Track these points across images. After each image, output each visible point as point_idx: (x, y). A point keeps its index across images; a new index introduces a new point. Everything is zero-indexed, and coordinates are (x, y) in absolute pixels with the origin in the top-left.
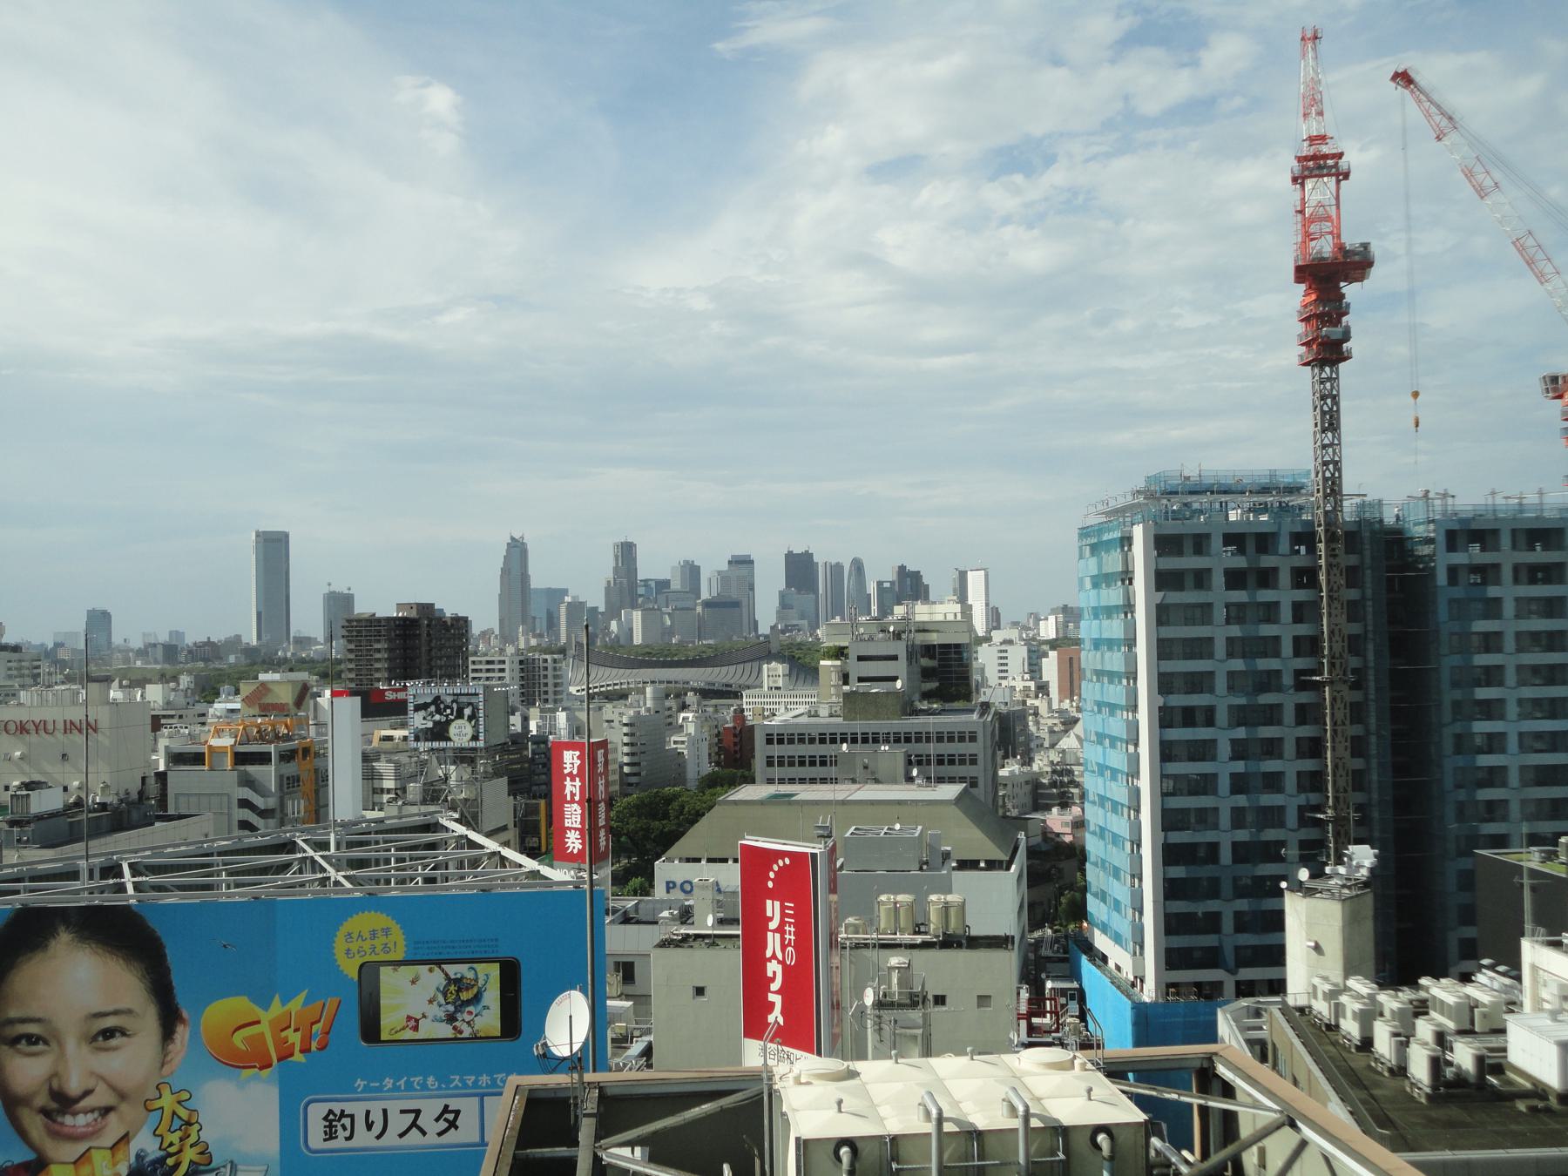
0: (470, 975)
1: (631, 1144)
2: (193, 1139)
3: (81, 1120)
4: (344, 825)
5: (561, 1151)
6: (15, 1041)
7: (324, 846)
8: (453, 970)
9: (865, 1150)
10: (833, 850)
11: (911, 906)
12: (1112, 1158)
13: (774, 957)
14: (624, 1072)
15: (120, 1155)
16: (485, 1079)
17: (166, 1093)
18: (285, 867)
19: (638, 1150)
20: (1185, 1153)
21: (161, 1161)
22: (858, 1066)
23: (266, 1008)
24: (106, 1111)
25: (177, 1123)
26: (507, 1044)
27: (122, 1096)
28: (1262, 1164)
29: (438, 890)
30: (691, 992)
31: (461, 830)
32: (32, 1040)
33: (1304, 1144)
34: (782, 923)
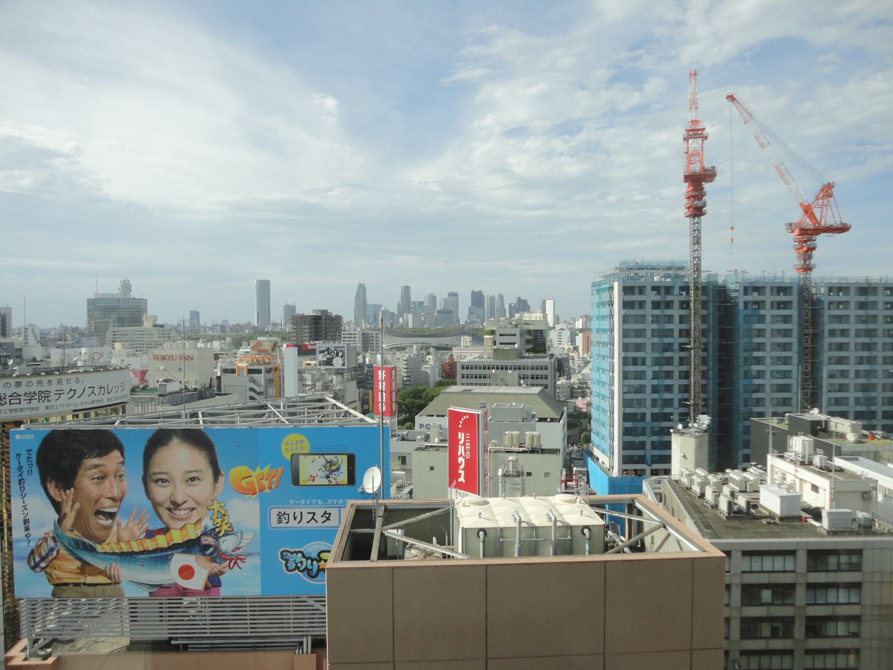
0: (335, 460)
1: (397, 528)
2: (226, 521)
3: (183, 512)
4: (287, 398)
5: (368, 530)
6: (157, 481)
7: (278, 407)
8: (329, 458)
9: (489, 533)
10: (486, 412)
11: (518, 436)
12: (590, 539)
13: (461, 455)
14: (397, 499)
15: (198, 527)
16: (341, 501)
17: (215, 503)
18: (264, 415)
19: (400, 531)
20: (622, 538)
21: (214, 530)
22: (489, 499)
23: (254, 471)
24: (193, 509)
25: (220, 515)
26: (350, 487)
27: (198, 504)
28: (652, 542)
29: (325, 425)
30: (428, 469)
31: (334, 401)
32: (163, 481)
33: (669, 535)
34: (465, 442)
